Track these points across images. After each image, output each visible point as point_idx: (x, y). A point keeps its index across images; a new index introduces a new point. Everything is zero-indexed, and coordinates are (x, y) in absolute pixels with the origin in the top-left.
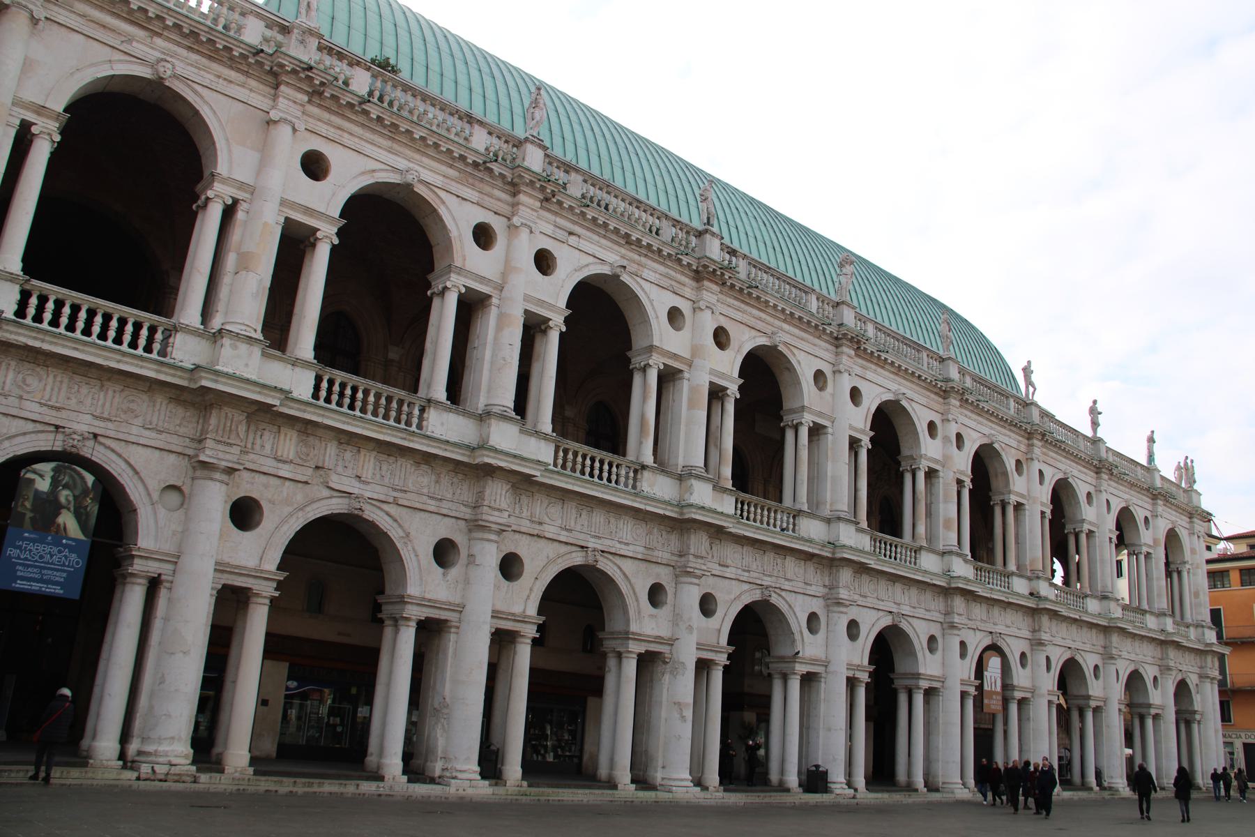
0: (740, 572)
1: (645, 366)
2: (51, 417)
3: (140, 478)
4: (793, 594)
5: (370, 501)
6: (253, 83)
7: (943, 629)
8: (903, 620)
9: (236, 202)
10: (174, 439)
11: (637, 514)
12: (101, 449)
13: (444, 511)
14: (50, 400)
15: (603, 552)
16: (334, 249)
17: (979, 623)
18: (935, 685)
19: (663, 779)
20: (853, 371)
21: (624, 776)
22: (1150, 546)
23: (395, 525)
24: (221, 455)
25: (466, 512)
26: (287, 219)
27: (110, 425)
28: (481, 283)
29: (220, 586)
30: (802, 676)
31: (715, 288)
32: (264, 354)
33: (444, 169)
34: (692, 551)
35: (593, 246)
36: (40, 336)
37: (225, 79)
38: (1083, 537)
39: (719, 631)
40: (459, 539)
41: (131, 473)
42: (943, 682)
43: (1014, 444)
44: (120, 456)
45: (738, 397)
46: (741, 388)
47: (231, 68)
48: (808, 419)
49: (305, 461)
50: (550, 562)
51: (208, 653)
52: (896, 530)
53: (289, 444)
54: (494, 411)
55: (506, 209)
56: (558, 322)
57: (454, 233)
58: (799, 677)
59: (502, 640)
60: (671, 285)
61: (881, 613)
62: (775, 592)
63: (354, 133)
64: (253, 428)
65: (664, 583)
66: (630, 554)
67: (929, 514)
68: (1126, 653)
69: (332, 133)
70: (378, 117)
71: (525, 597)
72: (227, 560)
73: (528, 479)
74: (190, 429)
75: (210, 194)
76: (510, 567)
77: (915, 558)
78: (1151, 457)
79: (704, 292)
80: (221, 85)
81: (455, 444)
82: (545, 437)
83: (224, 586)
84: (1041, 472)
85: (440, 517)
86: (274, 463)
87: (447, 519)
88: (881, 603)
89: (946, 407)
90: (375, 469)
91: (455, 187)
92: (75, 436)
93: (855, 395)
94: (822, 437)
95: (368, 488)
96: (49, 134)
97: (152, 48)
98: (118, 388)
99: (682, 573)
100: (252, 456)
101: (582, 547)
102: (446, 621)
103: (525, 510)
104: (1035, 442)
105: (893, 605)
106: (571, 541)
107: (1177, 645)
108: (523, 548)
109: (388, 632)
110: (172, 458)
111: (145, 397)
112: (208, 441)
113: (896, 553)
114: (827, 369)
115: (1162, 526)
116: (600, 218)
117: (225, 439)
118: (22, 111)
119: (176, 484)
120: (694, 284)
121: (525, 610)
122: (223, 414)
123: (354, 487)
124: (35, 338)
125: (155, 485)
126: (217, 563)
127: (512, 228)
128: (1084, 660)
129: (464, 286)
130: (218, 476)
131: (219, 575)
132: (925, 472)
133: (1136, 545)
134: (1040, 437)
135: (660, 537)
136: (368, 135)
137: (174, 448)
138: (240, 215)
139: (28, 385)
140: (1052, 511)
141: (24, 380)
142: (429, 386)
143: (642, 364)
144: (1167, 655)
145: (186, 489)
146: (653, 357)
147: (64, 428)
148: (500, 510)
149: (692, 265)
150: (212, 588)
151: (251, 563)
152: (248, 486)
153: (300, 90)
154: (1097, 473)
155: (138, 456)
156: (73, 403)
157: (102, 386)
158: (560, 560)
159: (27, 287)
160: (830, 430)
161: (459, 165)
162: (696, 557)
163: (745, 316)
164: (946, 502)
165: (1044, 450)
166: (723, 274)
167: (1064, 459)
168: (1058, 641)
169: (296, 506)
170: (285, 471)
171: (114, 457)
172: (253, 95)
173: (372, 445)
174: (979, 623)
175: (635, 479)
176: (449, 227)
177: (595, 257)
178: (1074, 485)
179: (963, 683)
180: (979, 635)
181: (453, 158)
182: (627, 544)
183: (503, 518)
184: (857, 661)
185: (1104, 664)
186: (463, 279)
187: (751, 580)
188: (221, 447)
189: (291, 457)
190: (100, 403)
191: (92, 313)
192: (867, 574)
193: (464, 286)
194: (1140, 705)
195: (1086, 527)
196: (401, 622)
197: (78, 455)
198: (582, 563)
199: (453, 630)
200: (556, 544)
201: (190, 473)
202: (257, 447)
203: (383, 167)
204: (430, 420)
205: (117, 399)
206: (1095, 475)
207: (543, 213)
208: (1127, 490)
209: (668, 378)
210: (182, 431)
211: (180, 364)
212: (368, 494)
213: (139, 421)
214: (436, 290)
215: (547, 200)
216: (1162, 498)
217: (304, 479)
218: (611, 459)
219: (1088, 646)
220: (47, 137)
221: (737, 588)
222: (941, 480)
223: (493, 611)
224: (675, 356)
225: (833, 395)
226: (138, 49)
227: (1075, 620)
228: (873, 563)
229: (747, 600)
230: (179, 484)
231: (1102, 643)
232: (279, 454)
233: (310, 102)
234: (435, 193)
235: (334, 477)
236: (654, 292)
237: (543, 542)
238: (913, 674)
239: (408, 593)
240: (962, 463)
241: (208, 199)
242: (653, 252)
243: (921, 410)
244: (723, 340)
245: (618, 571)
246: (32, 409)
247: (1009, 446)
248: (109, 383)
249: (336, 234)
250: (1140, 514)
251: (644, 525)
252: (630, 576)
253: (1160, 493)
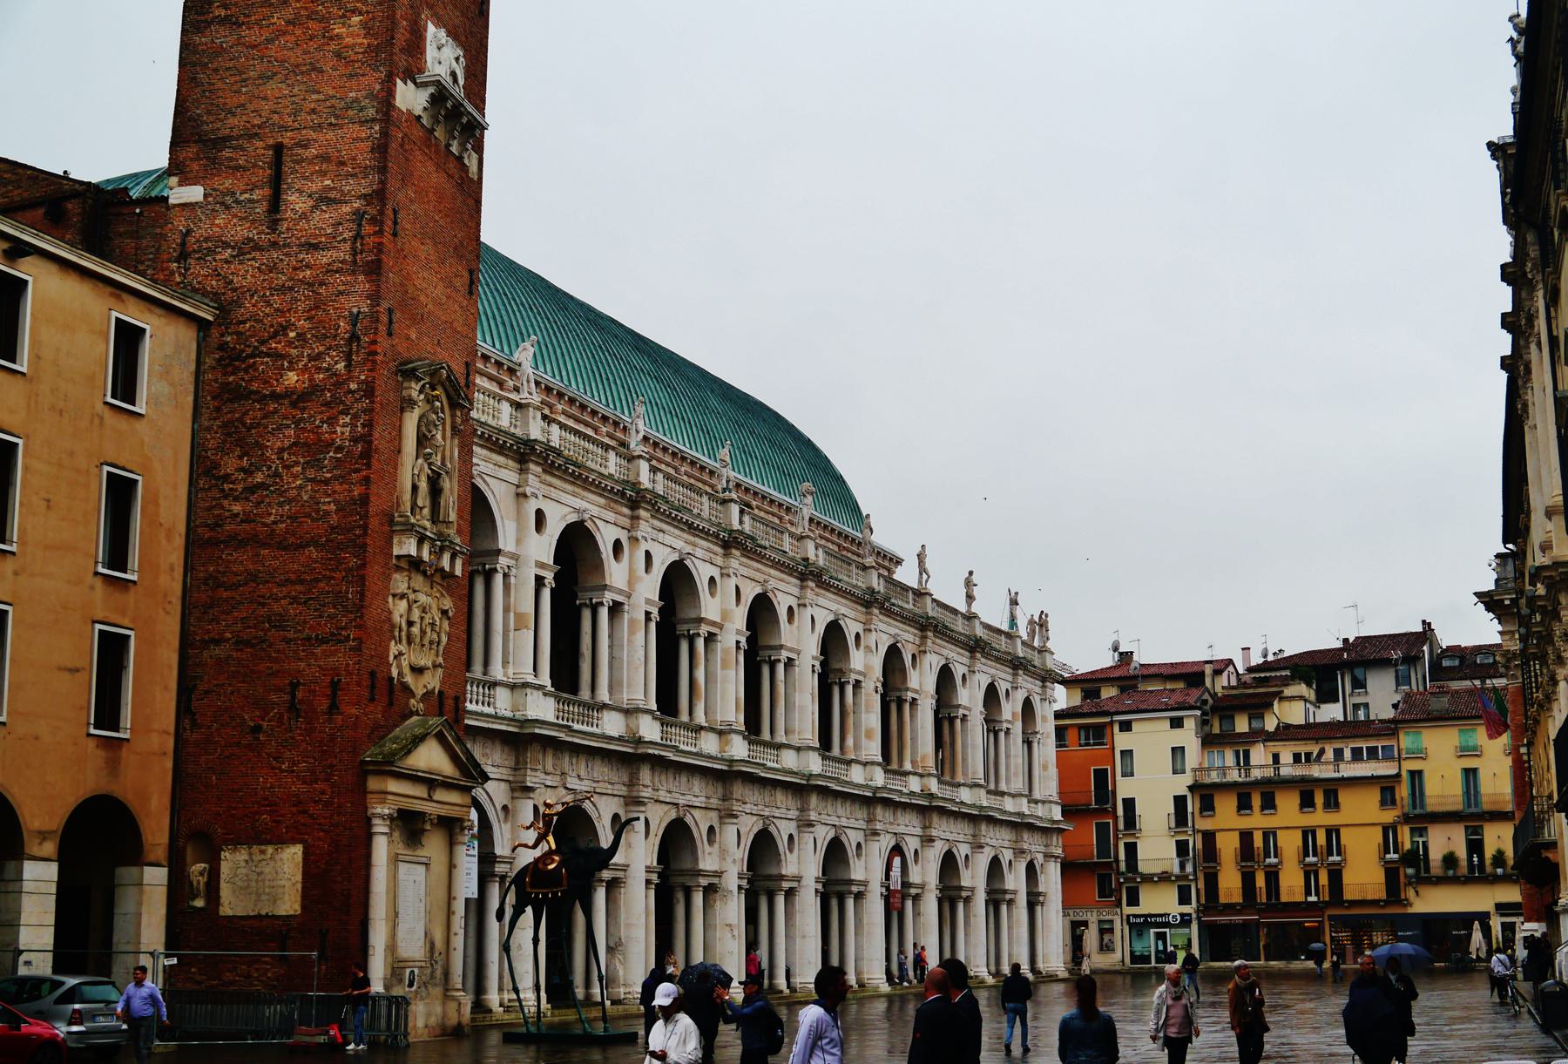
13: (615, 792)
25: (623, 790)
61: (829, 827)
95: (583, 783)
99: (728, 815)
105: (836, 818)
106: (672, 801)
107: (1031, 827)
144: (1022, 837)
182: (697, 796)
219: (961, 836)
229: (755, 830)
231: (972, 832)
235: (569, 779)
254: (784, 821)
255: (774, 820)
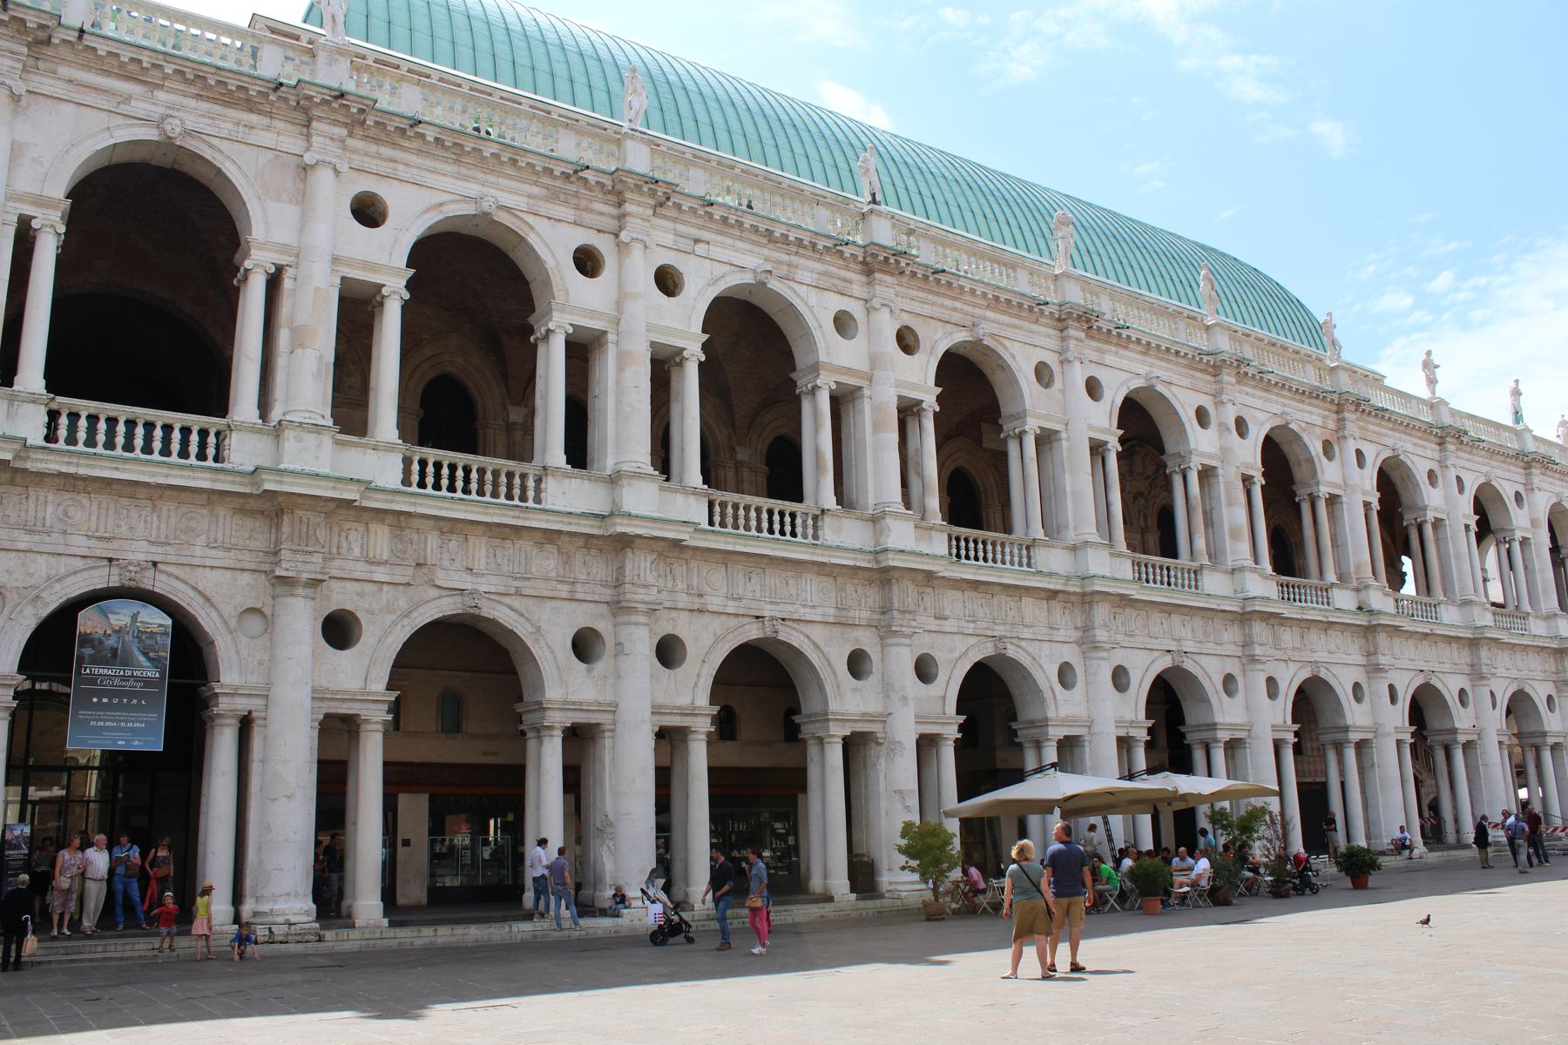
0: (963, 623)
1: (813, 388)
2: (101, 549)
3: (213, 605)
4: (1037, 642)
5: (486, 595)
6: (280, 125)
7: (1243, 665)
8: (1185, 659)
9: (280, 270)
10: (246, 556)
11: (821, 568)
12: (163, 577)
13: (580, 596)
14: (97, 530)
15: (783, 620)
16: (406, 308)
17: (1290, 653)
18: (1238, 735)
19: (890, 883)
20: (1087, 361)
21: (840, 883)
22: (1526, 530)
23: (521, 620)
24: (300, 567)
25: (606, 594)
26: (343, 278)
27: (169, 549)
28: (591, 318)
29: (321, 717)
30: (1059, 742)
31: (888, 279)
32: (337, 443)
33: (527, 188)
34: (896, 605)
35: (727, 252)
36: (75, 460)
37: (246, 126)
38: (1428, 529)
39: (944, 698)
40: (603, 626)
41: (201, 601)
42: (1249, 730)
43: (1319, 421)
44: (186, 583)
45: (938, 409)
46: (939, 399)
47: (251, 111)
48: (1032, 425)
49: (404, 559)
50: (718, 640)
51: (318, 794)
52: (1170, 549)
53: (381, 540)
54: (624, 469)
55: (611, 224)
56: (694, 351)
57: (550, 264)
58: (1055, 744)
59: (669, 739)
60: (834, 285)
61: (1156, 654)
62: (1012, 643)
63: (411, 162)
64: (336, 529)
65: (867, 649)
66: (819, 619)
67: (1209, 523)
68: (1504, 670)
69: (383, 167)
70: (437, 139)
71: (692, 686)
72: (325, 684)
73: (677, 544)
74: (261, 541)
75: (248, 264)
76: (668, 652)
77: (1196, 581)
78: (1517, 415)
79: (877, 287)
80: (242, 133)
81: (583, 515)
82: (695, 492)
83: (327, 716)
84: (1359, 453)
85: (574, 604)
86: (368, 567)
87: (584, 606)
88: (1154, 641)
89: (1218, 386)
90: (488, 557)
91: (543, 207)
92: (132, 568)
93: (1093, 388)
94: (1055, 445)
95: (484, 580)
96: (52, 226)
97: (154, 104)
98: (172, 505)
100: (338, 563)
101: (757, 617)
102: (598, 725)
103: (679, 583)
104: (1347, 415)
108: (683, 627)
109: (532, 744)
110: (246, 577)
111: (205, 512)
112: (283, 551)
113: (1169, 577)
114: (1052, 360)
115: (1541, 503)
116: (731, 216)
117: (303, 547)
118: (17, 205)
119: (254, 606)
120: (863, 279)
121: (693, 700)
122: (297, 519)
123: (467, 582)
124: (69, 463)
125: (229, 610)
126: (314, 690)
127: (622, 248)
128: (1444, 684)
129: (571, 325)
130: (300, 591)
131: (320, 704)
132: (1199, 472)
133: (1503, 530)
134: (1353, 408)
135: (854, 595)
136: (428, 163)
137: (247, 565)
138: (287, 283)
139: (69, 518)
140: (1380, 500)
141: (66, 513)
142: (544, 452)
143: (809, 386)
145: (267, 611)
146: (821, 376)
147: (118, 560)
148: (646, 586)
149: (857, 256)
150: (312, 720)
151: (354, 684)
152: (341, 598)
153: (336, 123)
154: (1439, 444)
155: (207, 580)
156: (124, 530)
157: (154, 506)
158: (730, 637)
159: (54, 406)
160: (1064, 435)
161: (546, 180)
162: (903, 612)
163: (934, 308)
164: (1230, 504)
165: (1361, 424)
166: (897, 262)
167: (1390, 432)
168: (1405, 663)
169: (399, 613)
170: (381, 574)
171: (179, 585)
172: (281, 138)
173: (481, 529)
174: (1290, 653)
175: (815, 527)
176: (543, 258)
177: (732, 265)
178: (1409, 463)
179: (1275, 728)
180: (1293, 667)
181: (537, 173)
183: (652, 595)
184: (1129, 716)
185: (1473, 686)
186: (569, 317)
187: (978, 632)
188: (299, 557)
189: (385, 558)
190: (154, 526)
191: (131, 424)
192: (1132, 607)
193: (571, 325)
194: (1531, 735)
195: (1430, 516)
196: (543, 733)
197: (138, 588)
198: (761, 636)
199: (607, 734)
200: (724, 618)
201: (269, 591)
202: (344, 551)
203: (451, 197)
204: (549, 491)
205: (173, 521)
206: (1438, 447)
207: (656, 221)
208: (1486, 461)
209: (841, 402)
210: (253, 544)
211: (240, 468)
212: (483, 588)
213: (202, 540)
214: (538, 335)
215: (661, 205)
216: (1539, 465)
217: (405, 580)
218: (782, 508)
220: (50, 230)
221: (961, 644)
222: (1221, 479)
223: (653, 707)
224: (848, 371)
225: (1063, 391)
226: (140, 107)
227: (1427, 634)
228: (1135, 592)
230: (259, 605)
232: (371, 555)
233: (351, 134)
234: (521, 219)
235: (440, 574)
236: (813, 297)
237: (706, 618)
238: (1208, 725)
239: (547, 696)
240: (1249, 455)
241: (247, 270)
242: (805, 247)
243: (1184, 396)
244: (910, 340)
245: (806, 640)
246: (80, 544)
247: (1310, 424)
248: (161, 502)
249: (406, 287)
250: (1507, 491)
251: (831, 580)
252: (821, 644)
253: (1533, 460)
254: (1046, 646)
255: (1023, 644)
